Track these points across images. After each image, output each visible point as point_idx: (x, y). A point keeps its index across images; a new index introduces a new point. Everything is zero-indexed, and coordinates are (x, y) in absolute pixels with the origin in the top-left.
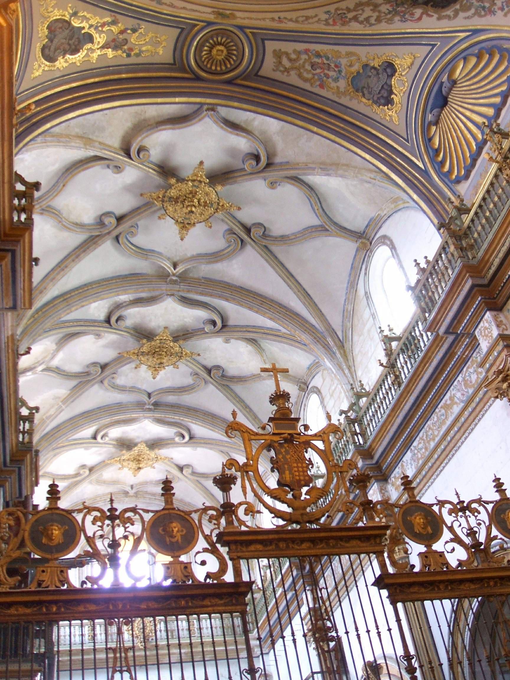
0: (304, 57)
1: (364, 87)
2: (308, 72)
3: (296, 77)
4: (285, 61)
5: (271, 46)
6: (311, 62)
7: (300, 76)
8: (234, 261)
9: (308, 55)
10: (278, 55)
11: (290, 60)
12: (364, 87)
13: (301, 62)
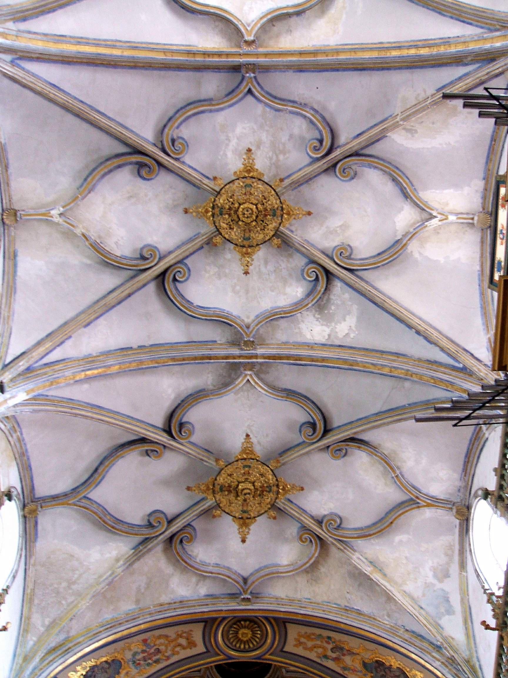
0: (169, 653)
1: (109, 668)
2: (161, 644)
3: (169, 634)
4: (183, 641)
5: (201, 648)
6: (161, 652)
7: (167, 637)
8: (173, 396)
9: (165, 656)
10: (192, 644)
11: (180, 645)
12: (109, 668)
13: (169, 648)
